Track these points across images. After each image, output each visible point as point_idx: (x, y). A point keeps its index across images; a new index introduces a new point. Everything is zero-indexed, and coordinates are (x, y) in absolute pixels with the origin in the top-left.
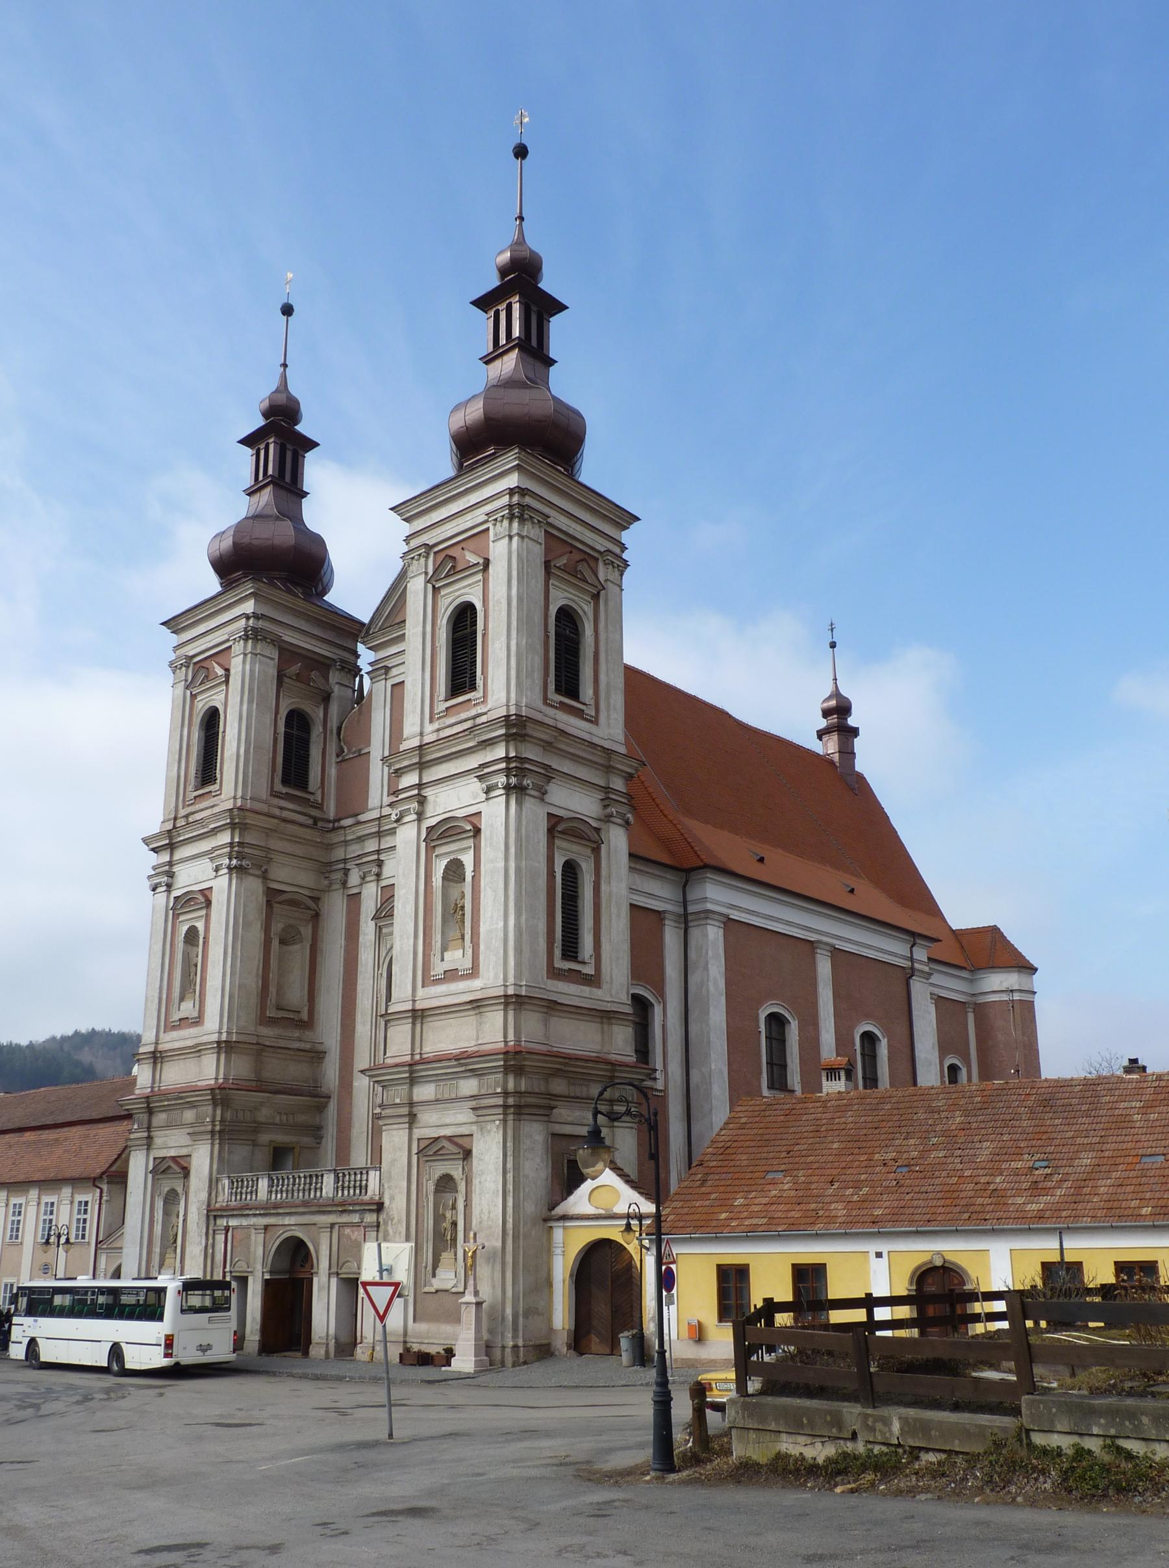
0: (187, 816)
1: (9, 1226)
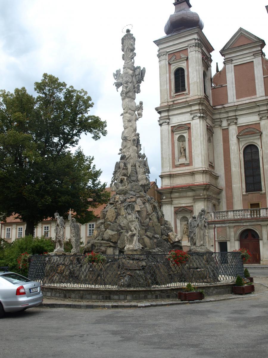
0: (173, 101)
1: (18, 234)
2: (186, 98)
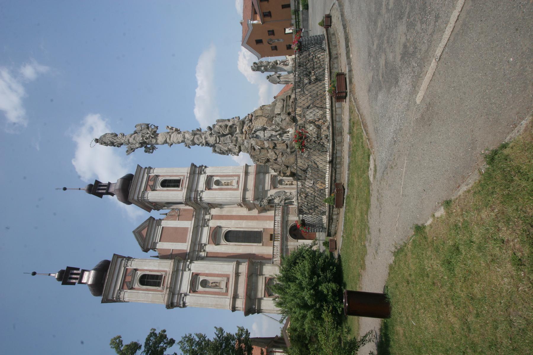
2: (169, 275)
